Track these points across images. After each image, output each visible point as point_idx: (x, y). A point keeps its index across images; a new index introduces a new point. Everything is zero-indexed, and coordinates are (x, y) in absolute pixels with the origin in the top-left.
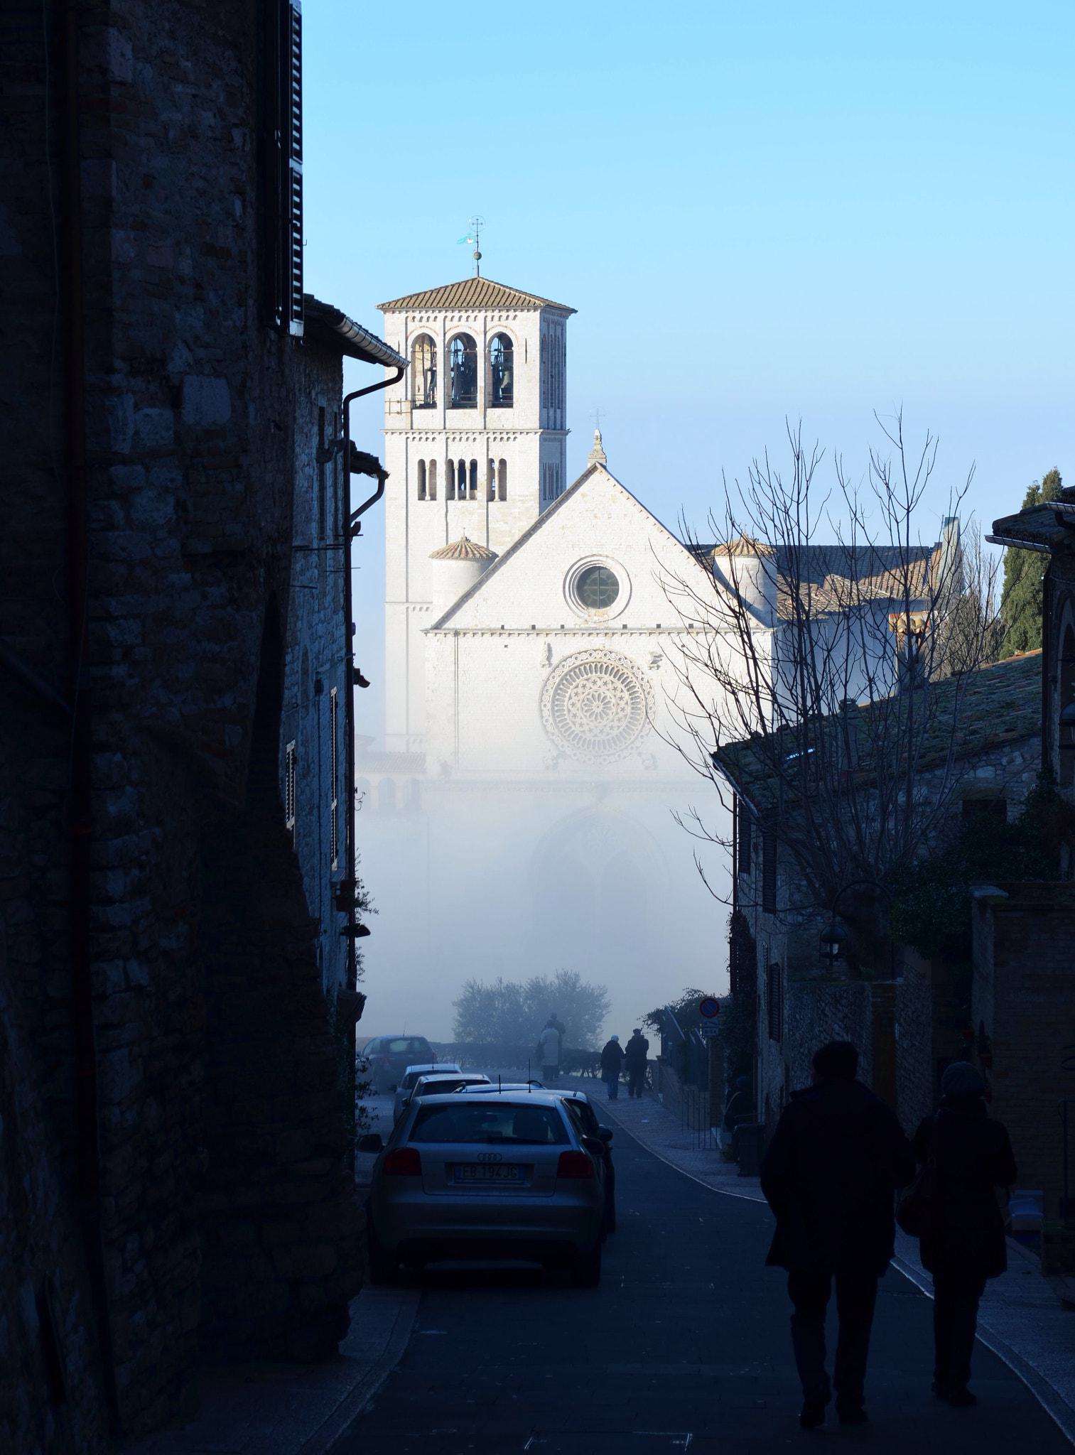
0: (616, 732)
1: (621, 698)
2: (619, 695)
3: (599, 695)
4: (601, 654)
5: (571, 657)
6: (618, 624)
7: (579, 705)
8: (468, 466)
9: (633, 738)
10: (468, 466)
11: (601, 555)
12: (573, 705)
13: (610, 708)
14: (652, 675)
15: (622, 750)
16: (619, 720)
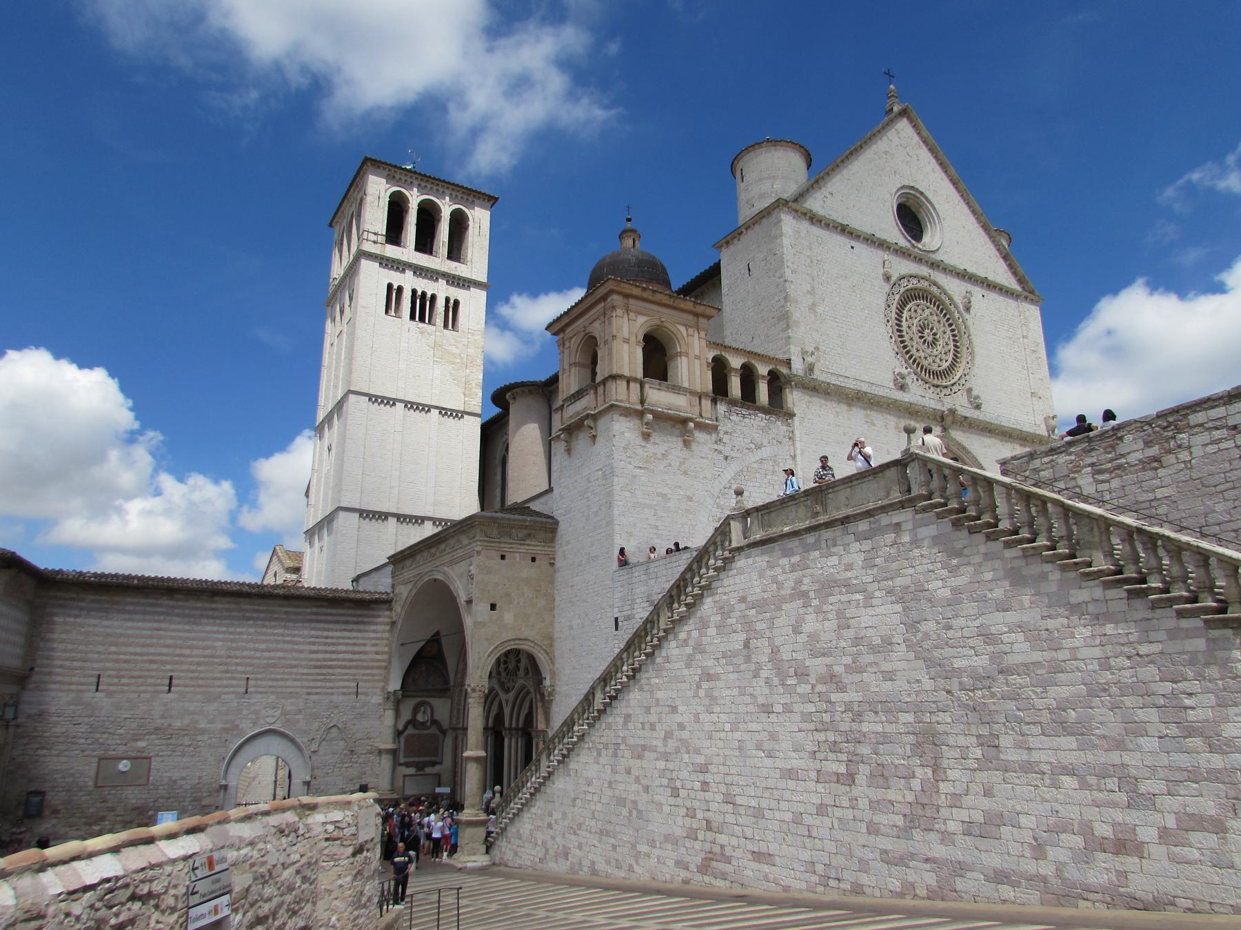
0: (945, 365)
1: (945, 333)
2: (942, 329)
3: (928, 325)
4: (926, 284)
5: (904, 278)
6: (938, 257)
7: (914, 329)
8: (429, 296)
9: (959, 375)
10: (429, 296)
11: (917, 190)
12: (909, 327)
13: (937, 341)
14: (966, 316)
15: (953, 385)
16: (945, 353)
